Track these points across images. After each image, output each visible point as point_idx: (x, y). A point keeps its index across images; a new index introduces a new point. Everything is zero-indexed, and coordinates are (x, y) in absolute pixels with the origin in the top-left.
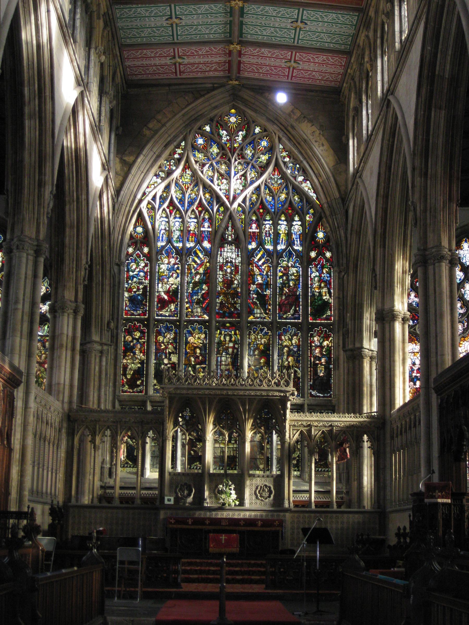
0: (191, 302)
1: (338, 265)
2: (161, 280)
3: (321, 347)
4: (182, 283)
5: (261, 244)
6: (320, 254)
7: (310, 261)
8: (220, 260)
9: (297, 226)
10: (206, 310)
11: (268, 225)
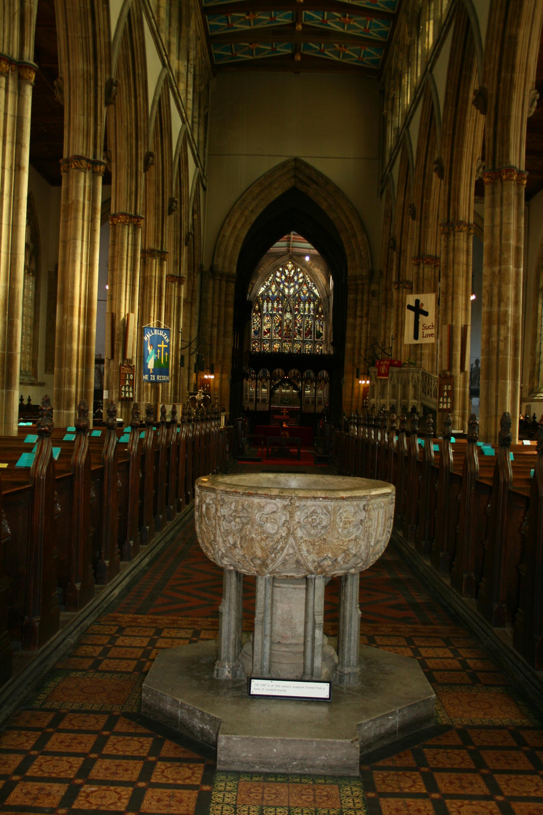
0: (275, 333)
1: (326, 321)
2: (264, 325)
3: (319, 349)
4: (272, 326)
5: (299, 312)
6: (320, 316)
7: (316, 318)
8: (285, 318)
9: (312, 306)
10: (280, 336)
11: (302, 305)
